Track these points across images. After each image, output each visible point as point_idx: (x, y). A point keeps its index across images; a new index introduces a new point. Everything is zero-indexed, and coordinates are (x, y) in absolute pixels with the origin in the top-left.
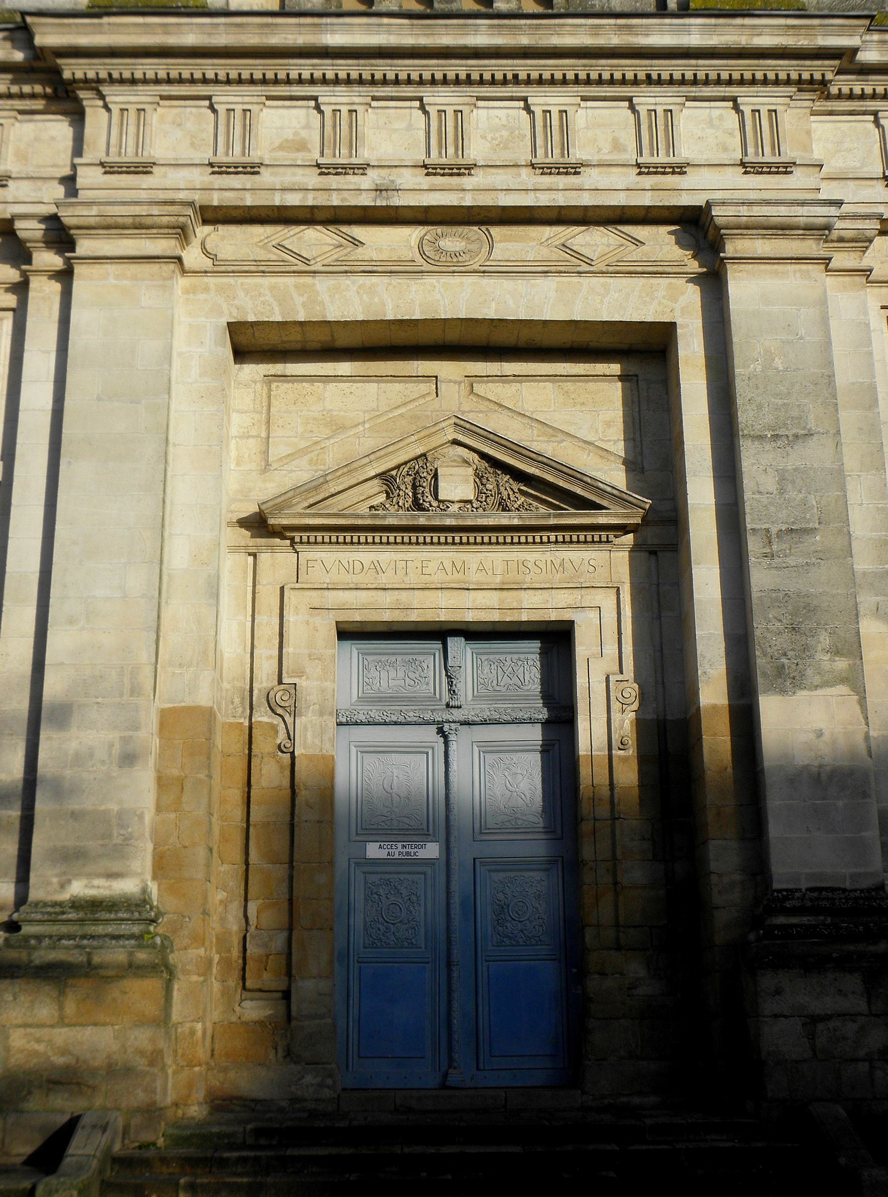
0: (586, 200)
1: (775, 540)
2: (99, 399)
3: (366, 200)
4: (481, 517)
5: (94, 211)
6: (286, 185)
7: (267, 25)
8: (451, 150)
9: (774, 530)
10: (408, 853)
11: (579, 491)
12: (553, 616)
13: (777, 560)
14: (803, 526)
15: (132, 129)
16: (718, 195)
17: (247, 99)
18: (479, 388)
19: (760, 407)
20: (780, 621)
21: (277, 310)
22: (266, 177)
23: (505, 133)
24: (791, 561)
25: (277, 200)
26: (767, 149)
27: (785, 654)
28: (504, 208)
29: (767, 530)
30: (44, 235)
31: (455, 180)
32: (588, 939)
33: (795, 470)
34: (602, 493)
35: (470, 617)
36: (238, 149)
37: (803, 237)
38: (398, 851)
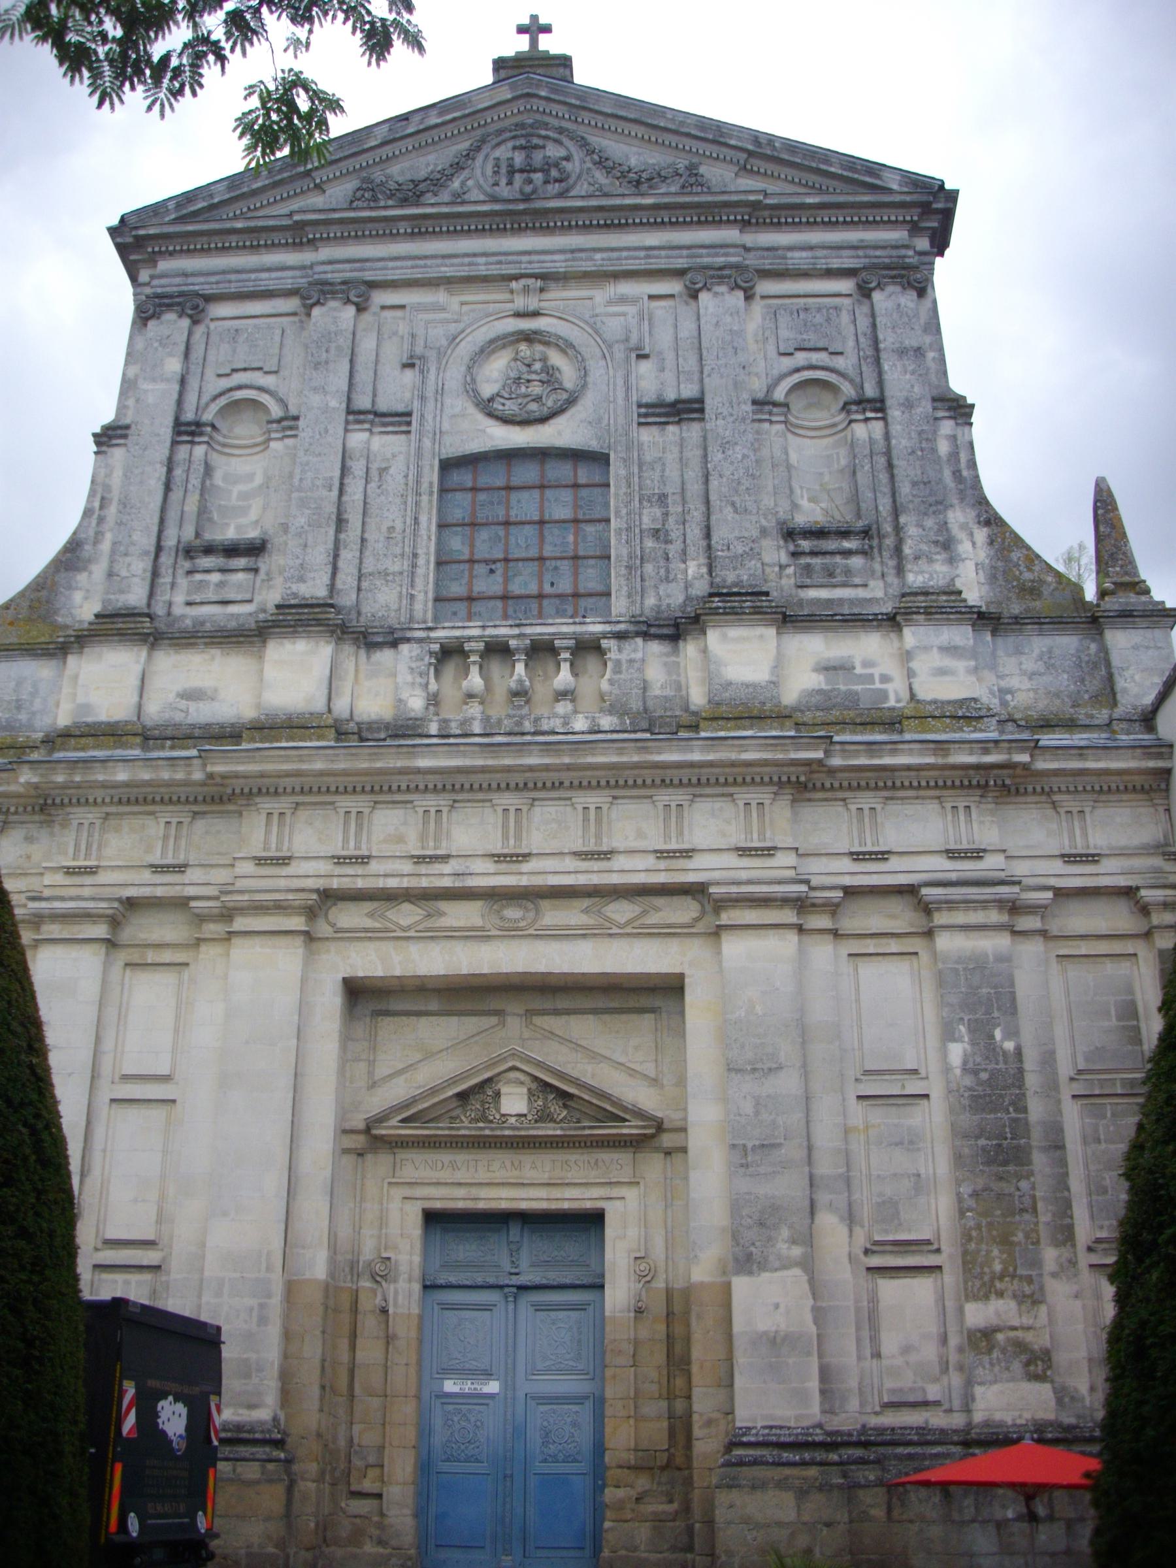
0: (615, 879)
3: (447, 882)
4: (533, 1128)
5: (246, 897)
6: (388, 872)
7: (375, 754)
8: (512, 842)
9: (750, 1145)
11: (609, 1108)
12: (588, 1205)
13: (751, 1169)
14: (772, 1141)
16: (716, 875)
17: (360, 804)
18: (538, 1020)
19: (743, 1046)
21: (380, 968)
22: (374, 867)
23: (554, 826)
24: (762, 1170)
25: (381, 883)
26: (755, 836)
27: (753, 1244)
28: (553, 886)
29: (744, 1146)
30: (216, 1454)
31: (514, 867)
32: (607, 1459)
33: (768, 1096)
34: (625, 1109)
35: (524, 1205)
36: (352, 844)
37: (781, 907)
38: (468, 1387)
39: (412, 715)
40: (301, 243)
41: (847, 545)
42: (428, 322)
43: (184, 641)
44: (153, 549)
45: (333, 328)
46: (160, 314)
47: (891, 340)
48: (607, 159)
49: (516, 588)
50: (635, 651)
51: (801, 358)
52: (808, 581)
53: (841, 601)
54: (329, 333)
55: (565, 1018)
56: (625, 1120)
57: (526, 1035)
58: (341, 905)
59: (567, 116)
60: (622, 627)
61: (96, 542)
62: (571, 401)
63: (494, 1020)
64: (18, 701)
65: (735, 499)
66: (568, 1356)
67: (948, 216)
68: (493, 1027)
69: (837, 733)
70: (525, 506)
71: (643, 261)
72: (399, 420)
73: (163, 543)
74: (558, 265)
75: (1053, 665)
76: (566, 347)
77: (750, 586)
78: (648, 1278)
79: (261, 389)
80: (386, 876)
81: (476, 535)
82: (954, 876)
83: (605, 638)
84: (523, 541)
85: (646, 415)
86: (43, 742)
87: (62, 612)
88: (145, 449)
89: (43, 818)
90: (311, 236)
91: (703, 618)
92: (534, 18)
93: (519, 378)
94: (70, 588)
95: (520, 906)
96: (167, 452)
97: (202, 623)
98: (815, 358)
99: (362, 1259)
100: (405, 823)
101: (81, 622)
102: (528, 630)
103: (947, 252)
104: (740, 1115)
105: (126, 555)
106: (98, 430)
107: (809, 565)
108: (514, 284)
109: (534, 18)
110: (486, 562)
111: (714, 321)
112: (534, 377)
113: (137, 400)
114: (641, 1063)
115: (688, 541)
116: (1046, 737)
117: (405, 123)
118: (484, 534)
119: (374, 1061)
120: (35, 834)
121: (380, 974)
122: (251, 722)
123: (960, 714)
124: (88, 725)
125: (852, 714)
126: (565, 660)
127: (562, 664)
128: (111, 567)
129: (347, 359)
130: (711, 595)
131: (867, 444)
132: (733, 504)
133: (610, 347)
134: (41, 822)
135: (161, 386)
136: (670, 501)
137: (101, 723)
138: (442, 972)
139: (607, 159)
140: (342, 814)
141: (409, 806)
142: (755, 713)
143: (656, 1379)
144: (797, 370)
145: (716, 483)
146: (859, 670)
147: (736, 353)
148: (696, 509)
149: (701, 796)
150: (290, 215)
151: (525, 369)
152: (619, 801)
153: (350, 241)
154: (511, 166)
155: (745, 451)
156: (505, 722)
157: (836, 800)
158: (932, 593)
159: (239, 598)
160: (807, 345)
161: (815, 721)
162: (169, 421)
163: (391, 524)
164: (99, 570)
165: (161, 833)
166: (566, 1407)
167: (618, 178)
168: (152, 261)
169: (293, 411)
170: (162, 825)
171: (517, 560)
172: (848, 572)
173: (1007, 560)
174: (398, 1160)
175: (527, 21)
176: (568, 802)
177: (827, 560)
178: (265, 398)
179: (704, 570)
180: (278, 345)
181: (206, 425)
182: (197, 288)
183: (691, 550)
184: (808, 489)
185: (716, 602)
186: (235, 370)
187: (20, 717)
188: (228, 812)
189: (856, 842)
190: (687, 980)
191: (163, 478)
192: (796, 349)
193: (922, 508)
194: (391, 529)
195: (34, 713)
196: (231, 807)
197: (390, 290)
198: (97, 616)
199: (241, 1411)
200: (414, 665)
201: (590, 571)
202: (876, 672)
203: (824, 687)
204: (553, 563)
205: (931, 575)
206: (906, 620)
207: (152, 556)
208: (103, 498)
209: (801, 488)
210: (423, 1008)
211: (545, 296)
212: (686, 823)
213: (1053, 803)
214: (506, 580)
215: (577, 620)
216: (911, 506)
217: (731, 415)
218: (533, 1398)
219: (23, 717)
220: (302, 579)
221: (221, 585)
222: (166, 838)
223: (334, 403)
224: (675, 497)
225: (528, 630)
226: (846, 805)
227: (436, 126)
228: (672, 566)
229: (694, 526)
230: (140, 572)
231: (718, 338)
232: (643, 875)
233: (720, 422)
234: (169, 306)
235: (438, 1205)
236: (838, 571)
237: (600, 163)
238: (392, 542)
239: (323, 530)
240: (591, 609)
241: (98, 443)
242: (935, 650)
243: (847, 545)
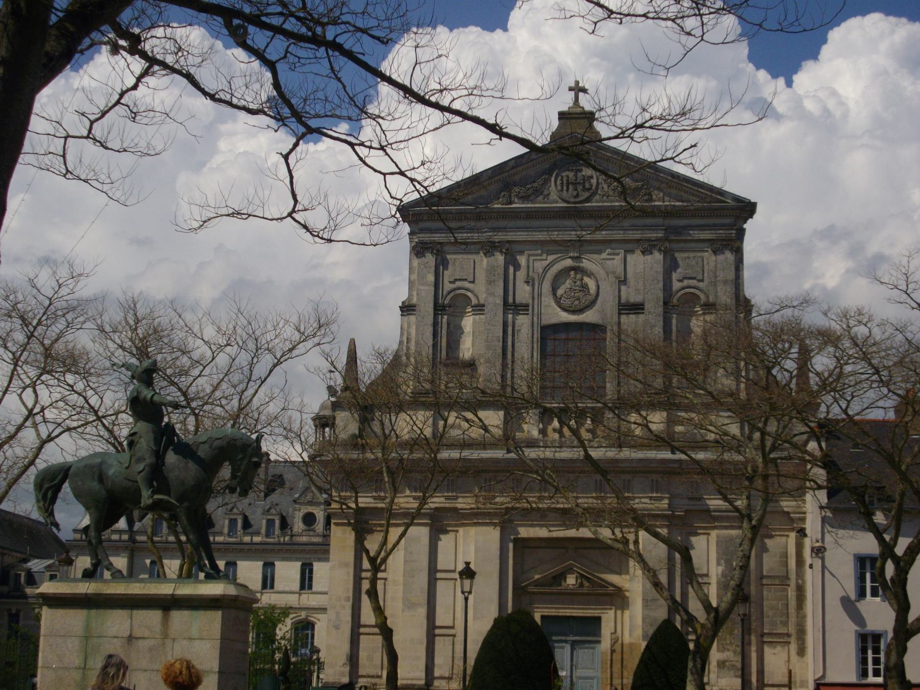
12: (596, 615)
35: (574, 615)
42: (534, 260)
51: (686, 282)
62: (593, 303)
76: (590, 275)
79: (467, 290)
92: (577, 83)
103: (755, 216)
109: (577, 83)
112: (577, 288)
121: (526, 536)
129: (502, 280)
133: (608, 275)
135: (427, 288)
151: (573, 284)
160: (688, 276)
162: (432, 305)
169: (482, 302)
175: (573, 85)
178: (469, 294)
186: (456, 280)
223: (498, 302)
227: (535, 159)
233: (650, 316)
234: (427, 248)
235: (546, 614)
241: (402, 311)
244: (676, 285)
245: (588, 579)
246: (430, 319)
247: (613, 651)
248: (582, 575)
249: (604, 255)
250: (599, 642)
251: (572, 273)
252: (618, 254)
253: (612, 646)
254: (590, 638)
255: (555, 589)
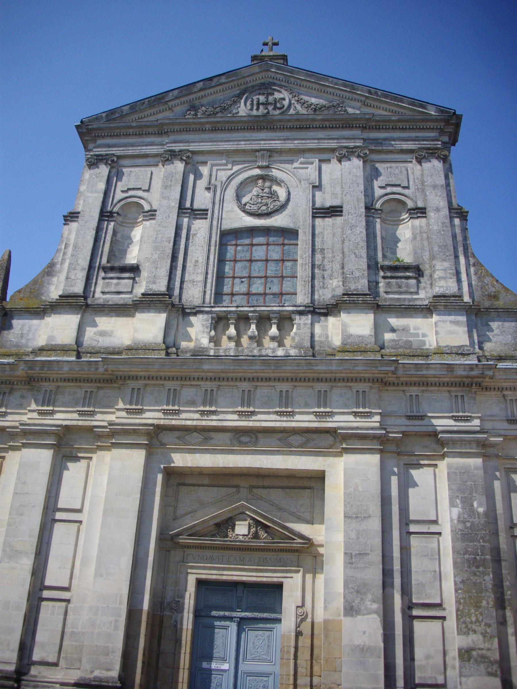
1: (354, 557)
2: (117, 495)
9: (354, 554)
10: (217, 667)
11: (287, 533)
12: (275, 580)
13: (354, 565)
14: (365, 552)
15: (135, 395)
18: (255, 490)
19: (352, 506)
20: (353, 589)
21: (181, 462)
23: (266, 399)
24: (359, 565)
28: (264, 427)
29: (351, 553)
33: (363, 530)
35: (244, 579)
39: (202, 346)
40: (162, 134)
41: (408, 274)
43: (99, 309)
44: (87, 267)
45: (174, 171)
46: (97, 163)
47: (430, 181)
48: (301, 99)
49: (254, 290)
50: (307, 319)
51: (389, 190)
52: (389, 290)
53: (404, 299)
54: (172, 173)
55: (268, 490)
56: (295, 540)
57: (249, 497)
58: (164, 432)
59: (284, 80)
60: (302, 308)
61: (62, 263)
63: (234, 490)
64: (22, 334)
65: (356, 251)
66: (262, 653)
67: (458, 126)
68: (234, 493)
69: (401, 360)
70: (259, 253)
71: (316, 145)
72: (202, 214)
73: (92, 265)
74: (278, 145)
75: (504, 331)
77: (362, 291)
78: (303, 617)
80: (186, 419)
81: (236, 265)
82: (455, 429)
83: (294, 313)
84: (257, 269)
85: (316, 213)
86: (32, 352)
87: (45, 294)
88: (87, 222)
89: (29, 387)
90: (166, 130)
91: (339, 305)
93: (258, 195)
94: (49, 284)
95: (248, 436)
96: (96, 224)
97: (108, 301)
98: (395, 189)
99: (166, 601)
100: (196, 395)
101: (53, 299)
102: (258, 309)
103: (457, 144)
104: (349, 539)
105: (75, 269)
106: (66, 214)
107: (390, 282)
108: (257, 153)
110: (241, 278)
111: (348, 172)
112: (265, 195)
113: (84, 201)
114: (304, 512)
115: (334, 270)
116: (501, 364)
117: (210, 82)
118: (239, 265)
119: (177, 507)
120: (25, 395)
121: (181, 465)
122: (127, 346)
123: (459, 352)
124: (52, 345)
125: (408, 351)
126: (274, 323)
127: (273, 325)
128: (67, 275)
129: (181, 184)
130: (344, 294)
131: (419, 228)
132: (355, 254)
133: (300, 182)
134: (28, 389)
135: (96, 195)
136: (326, 251)
137: (58, 345)
138: (210, 466)
139: (301, 99)
140: (167, 390)
141: (198, 387)
142: (362, 349)
143: (305, 667)
144: (387, 194)
145: (347, 244)
146: (412, 331)
147: (358, 186)
148: (338, 256)
149: (336, 386)
150: (157, 121)
151: (261, 191)
152: (297, 388)
153: (184, 133)
154: (258, 101)
155: (361, 230)
156: (245, 350)
157: (400, 390)
158: (448, 296)
159: (125, 290)
160: (391, 183)
161: (391, 354)
163: (196, 259)
164: (62, 276)
165: (83, 396)
166: (261, 678)
167: (306, 108)
168: (94, 140)
169: (155, 207)
170: (84, 392)
171: (254, 277)
172: (407, 286)
173: (483, 282)
174: (186, 554)
176: (273, 388)
177: (398, 280)
178: (142, 202)
179: (341, 283)
180: (149, 178)
181: (115, 213)
182: (114, 152)
183: (335, 274)
184: (390, 248)
185: (346, 298)
186: (129, 189)
187: (22, 341)
188: (114, 387)
189: (409, 410)
190: (326, 474)
191: (94, 236)
192: (386, 185)
193: (443, 257)
194: (197, 261)
195: (29, 340)
196: (116, 385)
197: (201, 155)
198: (60, 296)
199: (103, 672)
200: (204, 323)
201: (288, 283)
202: (420, 332)
203: (395, 338)
204: (271, 279)
205: (447, 288)
206: (435, 308)
207: (87, 270)
208: (66, 244)
209: (387, 248)
210: (201, 483)
211: (271, 159)
212: (328, 400)
213: (504, 396)
214: (249, 286)
215: (281, 305)
216: (438, 256)
217: (355, 213)
218: (245, 673)
219: (24, 341)
220: (154, 283)
221: (117, 284)
222: (85, 398)
224: (328, 250)
225: (258, 309)
226: (404, 393)
227: (224, 83)
228: (326, 281)
229: (336, 263)
230: (80, 277)
231: (350, 179)
232: (307, 423)
233: (350, 216)
234: (101, 160)
235: (203, 577)
236: (403, 285)
237: (298, 101)
238: (197, 267)
239: (165, 261)
240: (288, 300)
242: (448, 322)
243: (408, 274)
244: (378, 192)
245: (265, 527)
246: (94, 223)
247: (298, 634)
248: (258, 523)
249: (296, 165)
250: (279, 621)
251: (260, 181)
252: (312, 163)
253: (298, 626)
254: (265, 615)
255: (218, 541)
